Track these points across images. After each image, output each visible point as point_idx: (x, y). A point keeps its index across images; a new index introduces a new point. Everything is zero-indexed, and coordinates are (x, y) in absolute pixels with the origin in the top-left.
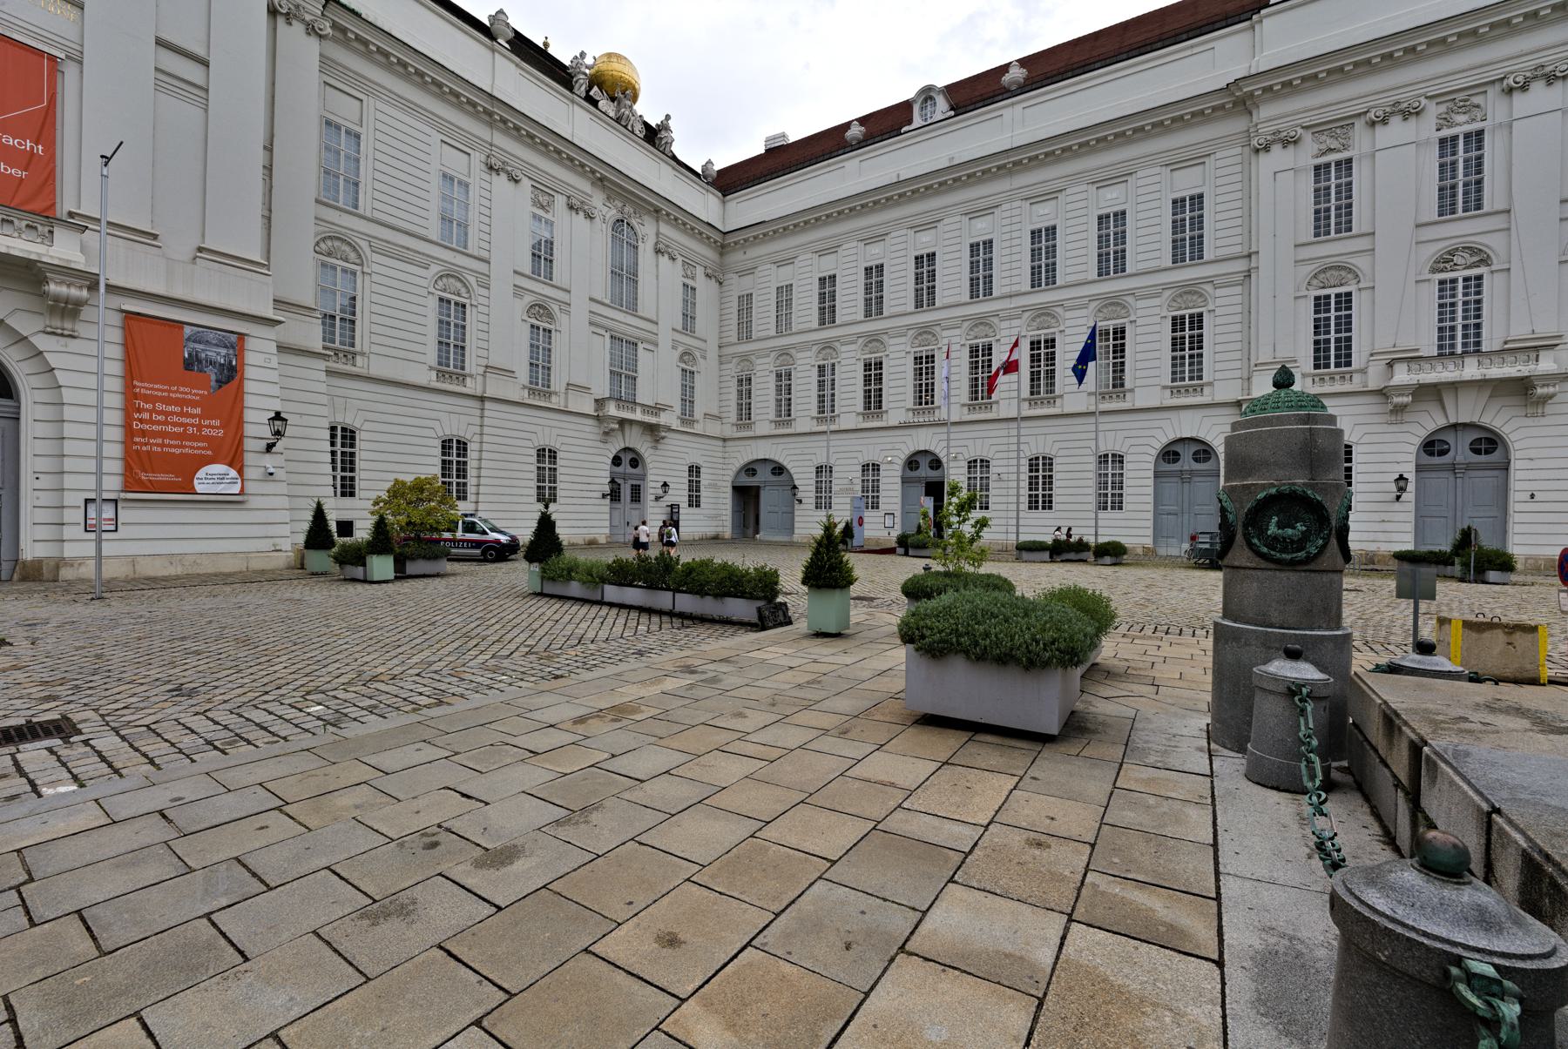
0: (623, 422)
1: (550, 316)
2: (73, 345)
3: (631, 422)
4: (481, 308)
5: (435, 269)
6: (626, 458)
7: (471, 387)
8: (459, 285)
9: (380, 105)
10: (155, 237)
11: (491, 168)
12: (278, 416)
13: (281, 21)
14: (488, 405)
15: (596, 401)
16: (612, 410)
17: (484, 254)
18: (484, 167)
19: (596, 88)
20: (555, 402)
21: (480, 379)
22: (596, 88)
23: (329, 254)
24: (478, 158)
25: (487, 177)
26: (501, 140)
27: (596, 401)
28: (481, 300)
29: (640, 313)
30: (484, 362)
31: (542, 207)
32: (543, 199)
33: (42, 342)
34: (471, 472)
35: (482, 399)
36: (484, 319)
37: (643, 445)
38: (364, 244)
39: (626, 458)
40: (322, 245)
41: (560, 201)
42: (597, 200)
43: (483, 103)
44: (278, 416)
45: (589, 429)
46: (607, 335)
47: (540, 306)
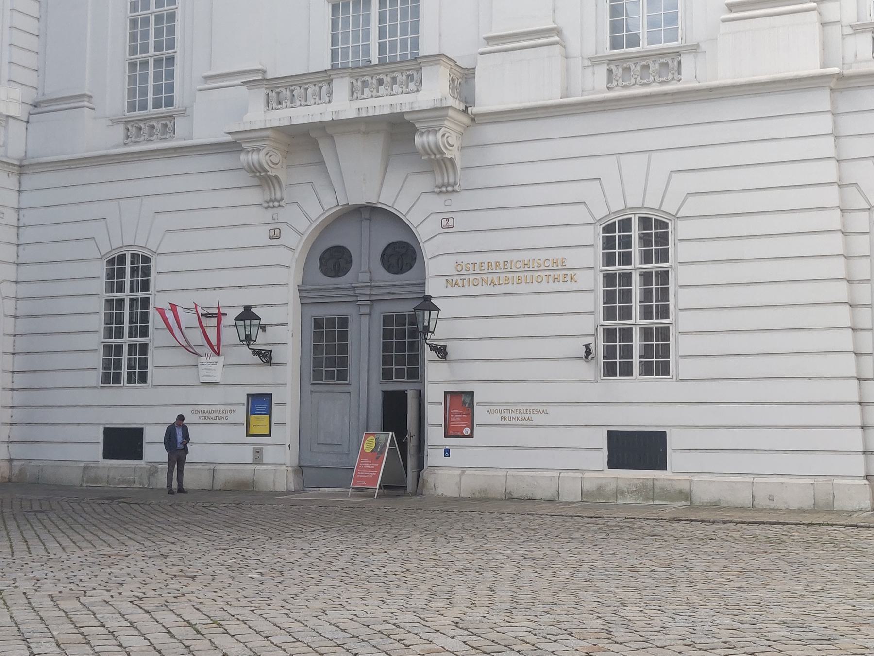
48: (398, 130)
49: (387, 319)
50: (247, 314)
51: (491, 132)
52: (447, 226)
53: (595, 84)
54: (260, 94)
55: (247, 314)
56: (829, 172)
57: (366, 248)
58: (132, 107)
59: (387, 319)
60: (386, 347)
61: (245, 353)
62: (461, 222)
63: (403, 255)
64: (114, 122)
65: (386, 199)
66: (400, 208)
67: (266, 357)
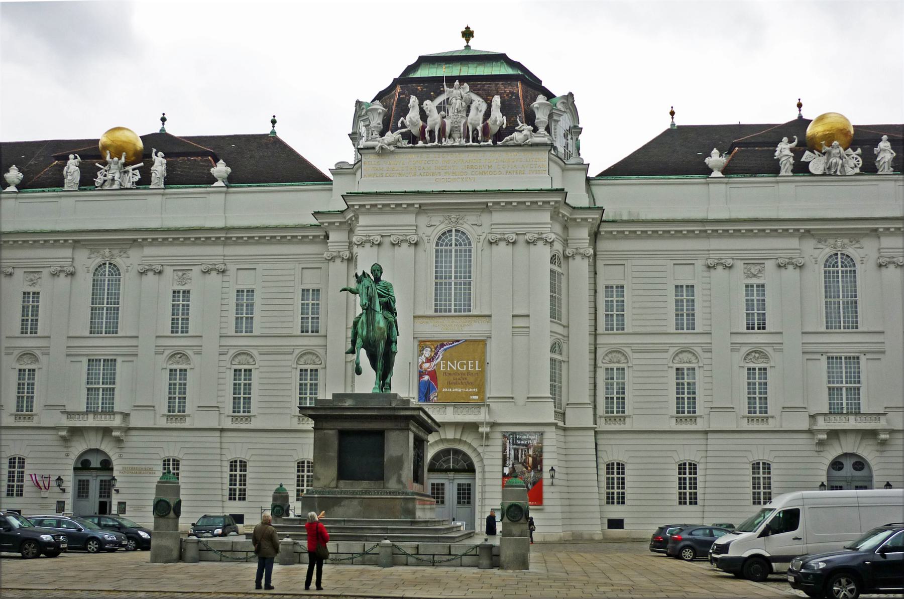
0: (834, 434)
1: (765, 356)
2: (488, 449)
3: (845, 431)
4: (706, 368)
5: (672, 351)
6: (848, 464)
7: (700, 425)
8: (690, 356)
9: (635, 262)
10: (512, 398)
11: (709, 267)
12: (552, 469)
13: (570, 260)
14: (710, 436)
15: (810, 416)
16: (821, 424)
17: (707, 329)
18: (705, 268)
19: (807, 153)
20: (772, 425)
21: (706, 417)
22: (807, 153)
23: (611, 362)
24: (700, 264)
25: (706, 274)
26: (715, 244)
27: (810, 416)
28: (707, 361)
29: (860, 329)
30: (710, 405)
31: (755, 276)
32: (754, 270)
33: (480, 450)
34: (699, 485)
35: (706, 432)
36: (708, 374)
37: (867, 452)
38: (628, 350)
39: (848, 464)
40: (607, 358)
41: (770, 265)
42: (809, 246)
43: (696, 228)
44: (552, 469)
45: (804, 443)
46: (824, 359)
47: (755, 352)
48: (106, 431)
49: (101, 481)
50: (59, 479)
51: (133, 433)
52: (120, 457)
53: (163, 423)
54: (65, 416)
55: (59, 479)
56: (218, 451)
57: (95, 462)
58: (18, 410)
59: (101, 481)
60: (101, 489)
61: (58, 489)
62: (124, 456)
63: (106, 465)
64: (11, 415)
65: (103, 448)
66: (106, 451)
67: (64, 491)
